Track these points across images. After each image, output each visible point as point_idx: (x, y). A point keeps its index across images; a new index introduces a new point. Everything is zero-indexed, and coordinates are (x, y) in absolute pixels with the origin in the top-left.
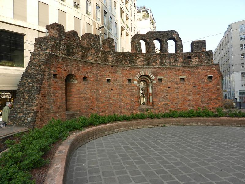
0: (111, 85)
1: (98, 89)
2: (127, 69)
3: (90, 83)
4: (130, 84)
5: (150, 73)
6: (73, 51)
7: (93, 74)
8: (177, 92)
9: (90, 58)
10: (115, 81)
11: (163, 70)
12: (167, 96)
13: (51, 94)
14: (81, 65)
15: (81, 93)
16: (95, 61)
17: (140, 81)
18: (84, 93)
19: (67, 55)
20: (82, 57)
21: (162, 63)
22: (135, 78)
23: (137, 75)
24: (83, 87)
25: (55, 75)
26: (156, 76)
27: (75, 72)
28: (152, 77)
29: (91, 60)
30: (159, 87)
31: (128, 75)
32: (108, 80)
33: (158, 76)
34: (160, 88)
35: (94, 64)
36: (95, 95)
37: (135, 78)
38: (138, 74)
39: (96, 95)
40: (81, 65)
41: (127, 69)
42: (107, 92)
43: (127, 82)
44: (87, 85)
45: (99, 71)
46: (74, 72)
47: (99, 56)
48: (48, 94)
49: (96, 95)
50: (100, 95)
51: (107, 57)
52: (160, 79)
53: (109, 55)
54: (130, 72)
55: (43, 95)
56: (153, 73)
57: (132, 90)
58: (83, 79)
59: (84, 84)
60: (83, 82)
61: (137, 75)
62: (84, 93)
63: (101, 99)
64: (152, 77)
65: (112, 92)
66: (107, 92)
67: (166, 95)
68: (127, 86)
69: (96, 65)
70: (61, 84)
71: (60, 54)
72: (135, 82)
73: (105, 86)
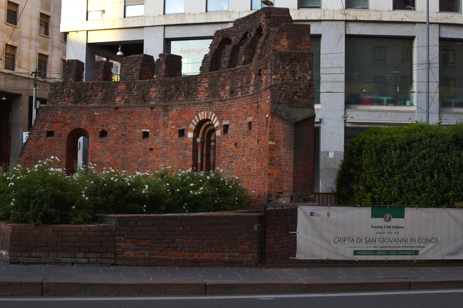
0: (148, 143)
1: (125, 150)
2: (177, 110)
3: (110, 140)
4: (181, 139)
5: (214, 115)
6: (86, 95)
7: (118, 126)
8: (243, 156)
9: (118, 99)
10: (156, 134)
11: (231, 105)
12: (232, 164)
13: (40, 157)
14: (97, 114)
15: (95, 156)
16: (125, 102)
17: (207, 131)
18: (100, 156)
19: (76, 102)
20: (103, 99)
21: (232, 92)
22: (191, 126)
23: (193, 121)
24: (99, 147)
25: (50, 134)
26: (220, 120)
27: (84, 125)
28: (216, 122)
29: (119, 101)
30: (223, 143)
31: (179, 122)
32: (146, 135)
33: (223, 119)
34: (225, 146)
35: (120, 109)
36: (120, 159)
37: (190, 126)
38: (196, 117)
39: (123, 159)
40: (97, 114)
41: (177, 110)
42: (141, 154)
43: (177, 136)
44: (106, 142)
45: (130, 119)
46: (84, 124)
47: (133, 93)
48: (35, 157)
49: (123, 159)
50: (128, 159)
51: (148, 93)
52: (226, 127)
53: (151, 87)
54: (183, 116)
55: (27, 158)
56: (218, 114)
57: (184, 151)
58: (99, 134)
59: (100, 142)
60: (99, 140)
61: (193, 121)
62: (100, 156)
63: (132, 166)
64: (216, 122)
65: (151, 154)
66: (141, 154)
67: (232, 162)
68: (176, 142)
69: (123, 109)
70: (59, 143)
71: (61, 103)
72: (190, 135)
73: (139, 143)
